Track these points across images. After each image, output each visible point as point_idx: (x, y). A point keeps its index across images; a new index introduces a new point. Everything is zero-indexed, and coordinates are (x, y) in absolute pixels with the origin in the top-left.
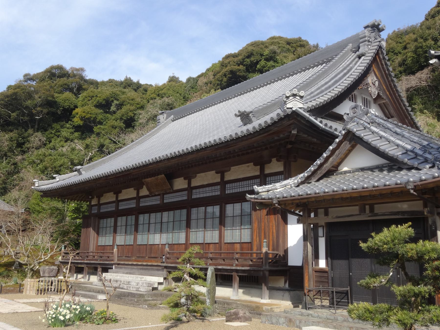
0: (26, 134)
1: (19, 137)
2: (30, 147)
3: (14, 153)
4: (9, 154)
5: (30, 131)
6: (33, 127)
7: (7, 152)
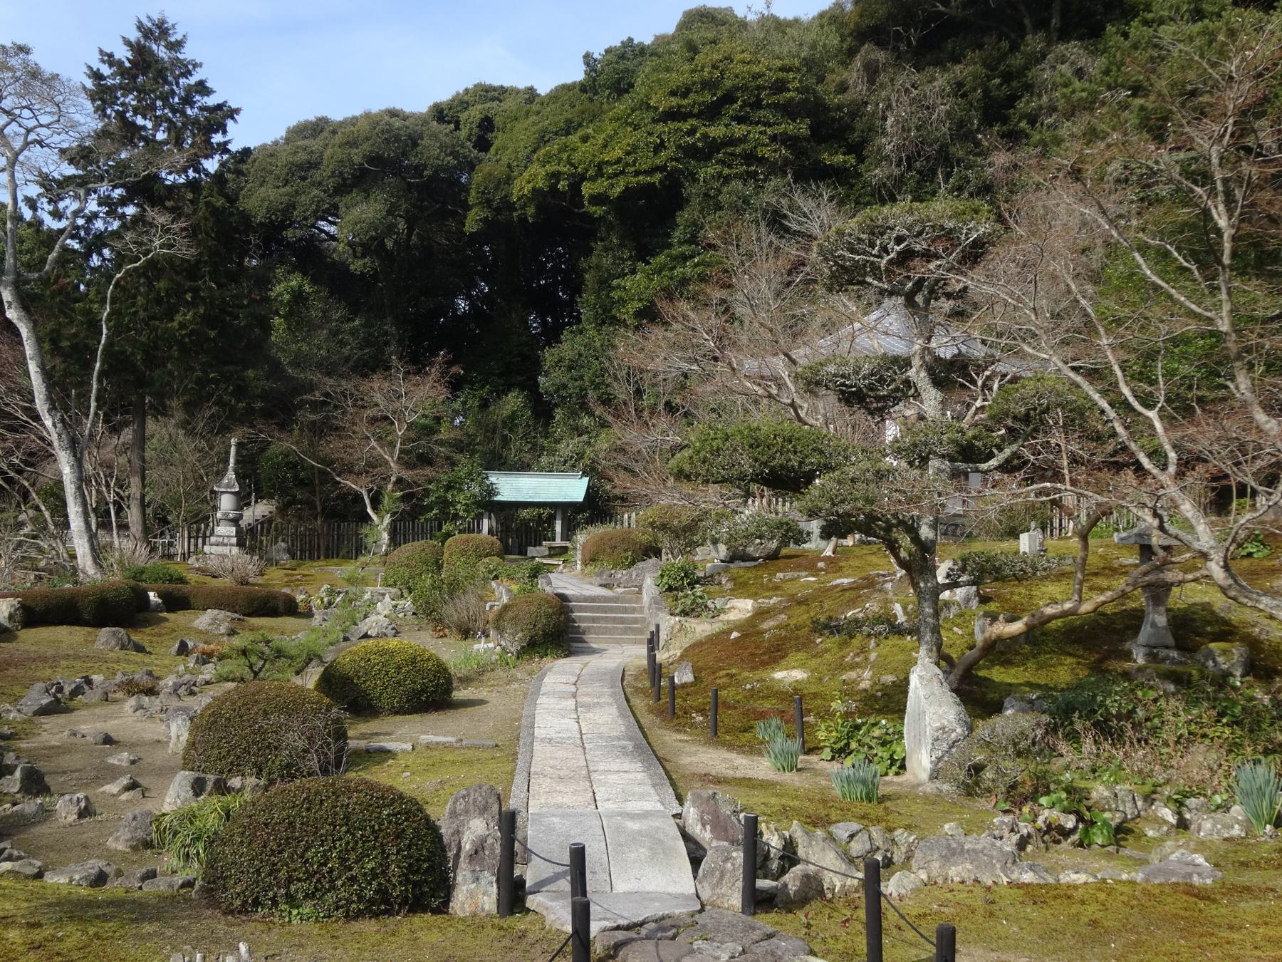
0: (1017, 61)
1: (989, 78)
2: (1041, 108)
3: (978, 144)
4: (958, 151)
5: (1034, 42)
6: (1041, 25)
7: (947, 145)
